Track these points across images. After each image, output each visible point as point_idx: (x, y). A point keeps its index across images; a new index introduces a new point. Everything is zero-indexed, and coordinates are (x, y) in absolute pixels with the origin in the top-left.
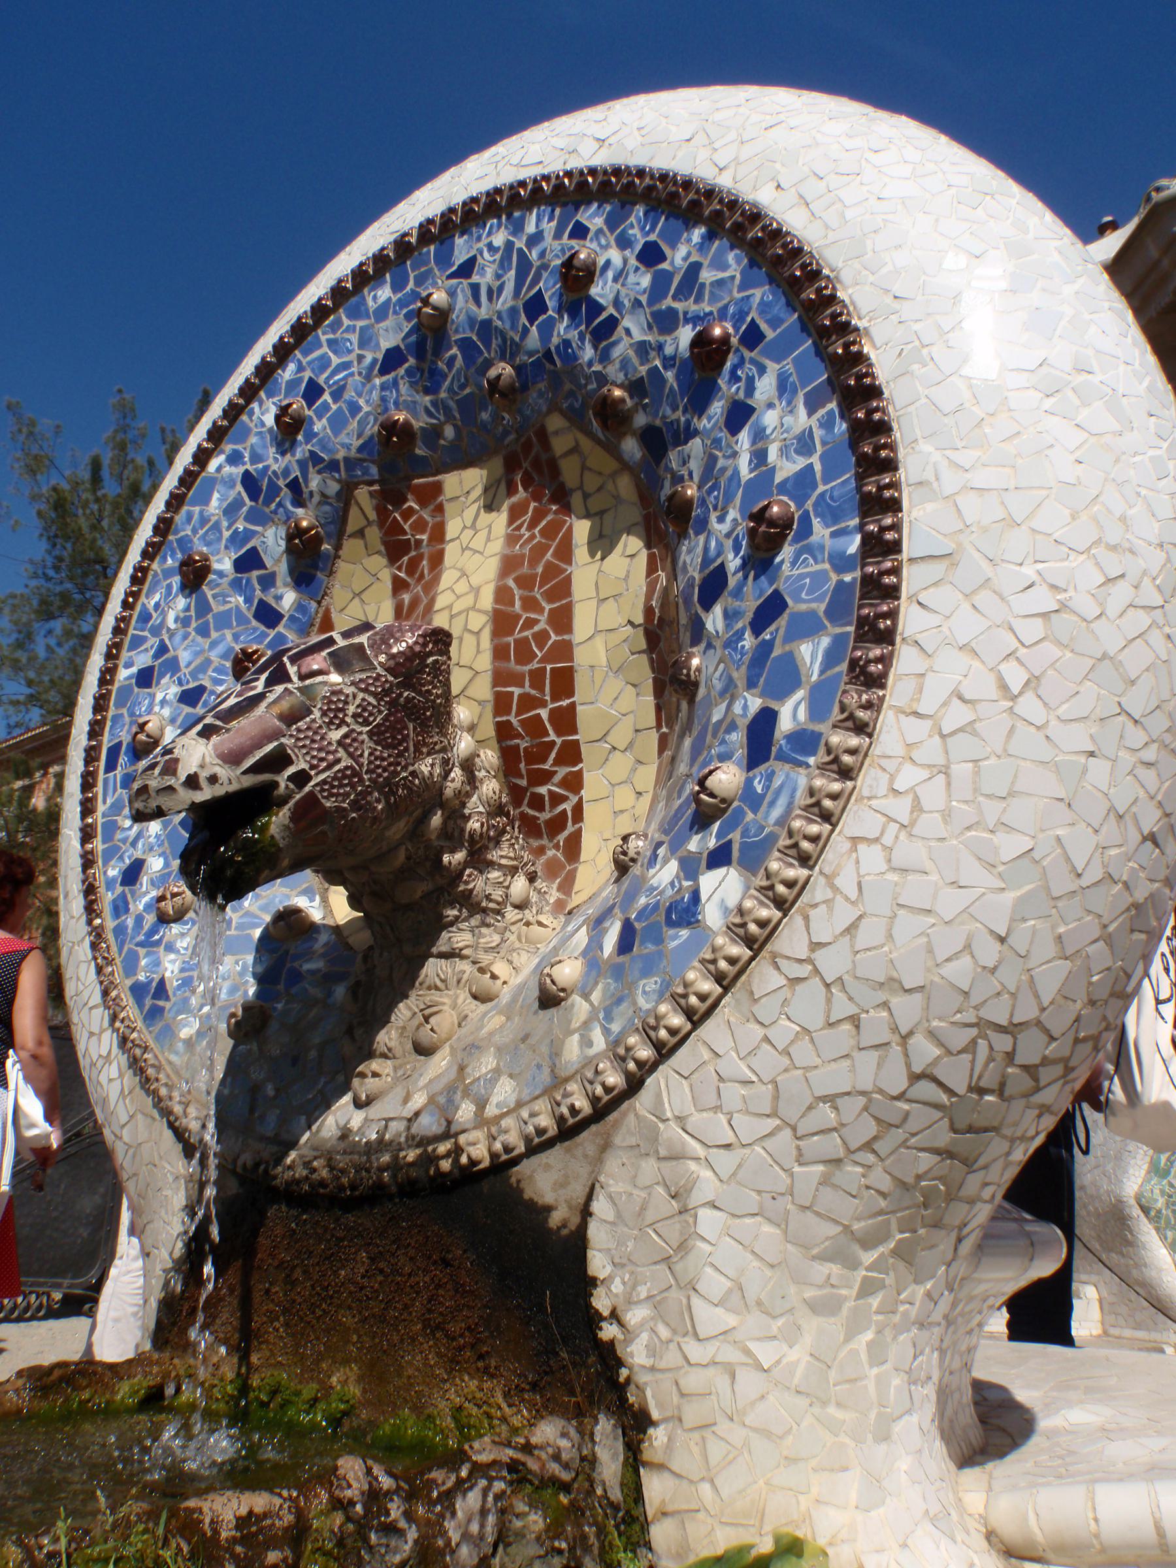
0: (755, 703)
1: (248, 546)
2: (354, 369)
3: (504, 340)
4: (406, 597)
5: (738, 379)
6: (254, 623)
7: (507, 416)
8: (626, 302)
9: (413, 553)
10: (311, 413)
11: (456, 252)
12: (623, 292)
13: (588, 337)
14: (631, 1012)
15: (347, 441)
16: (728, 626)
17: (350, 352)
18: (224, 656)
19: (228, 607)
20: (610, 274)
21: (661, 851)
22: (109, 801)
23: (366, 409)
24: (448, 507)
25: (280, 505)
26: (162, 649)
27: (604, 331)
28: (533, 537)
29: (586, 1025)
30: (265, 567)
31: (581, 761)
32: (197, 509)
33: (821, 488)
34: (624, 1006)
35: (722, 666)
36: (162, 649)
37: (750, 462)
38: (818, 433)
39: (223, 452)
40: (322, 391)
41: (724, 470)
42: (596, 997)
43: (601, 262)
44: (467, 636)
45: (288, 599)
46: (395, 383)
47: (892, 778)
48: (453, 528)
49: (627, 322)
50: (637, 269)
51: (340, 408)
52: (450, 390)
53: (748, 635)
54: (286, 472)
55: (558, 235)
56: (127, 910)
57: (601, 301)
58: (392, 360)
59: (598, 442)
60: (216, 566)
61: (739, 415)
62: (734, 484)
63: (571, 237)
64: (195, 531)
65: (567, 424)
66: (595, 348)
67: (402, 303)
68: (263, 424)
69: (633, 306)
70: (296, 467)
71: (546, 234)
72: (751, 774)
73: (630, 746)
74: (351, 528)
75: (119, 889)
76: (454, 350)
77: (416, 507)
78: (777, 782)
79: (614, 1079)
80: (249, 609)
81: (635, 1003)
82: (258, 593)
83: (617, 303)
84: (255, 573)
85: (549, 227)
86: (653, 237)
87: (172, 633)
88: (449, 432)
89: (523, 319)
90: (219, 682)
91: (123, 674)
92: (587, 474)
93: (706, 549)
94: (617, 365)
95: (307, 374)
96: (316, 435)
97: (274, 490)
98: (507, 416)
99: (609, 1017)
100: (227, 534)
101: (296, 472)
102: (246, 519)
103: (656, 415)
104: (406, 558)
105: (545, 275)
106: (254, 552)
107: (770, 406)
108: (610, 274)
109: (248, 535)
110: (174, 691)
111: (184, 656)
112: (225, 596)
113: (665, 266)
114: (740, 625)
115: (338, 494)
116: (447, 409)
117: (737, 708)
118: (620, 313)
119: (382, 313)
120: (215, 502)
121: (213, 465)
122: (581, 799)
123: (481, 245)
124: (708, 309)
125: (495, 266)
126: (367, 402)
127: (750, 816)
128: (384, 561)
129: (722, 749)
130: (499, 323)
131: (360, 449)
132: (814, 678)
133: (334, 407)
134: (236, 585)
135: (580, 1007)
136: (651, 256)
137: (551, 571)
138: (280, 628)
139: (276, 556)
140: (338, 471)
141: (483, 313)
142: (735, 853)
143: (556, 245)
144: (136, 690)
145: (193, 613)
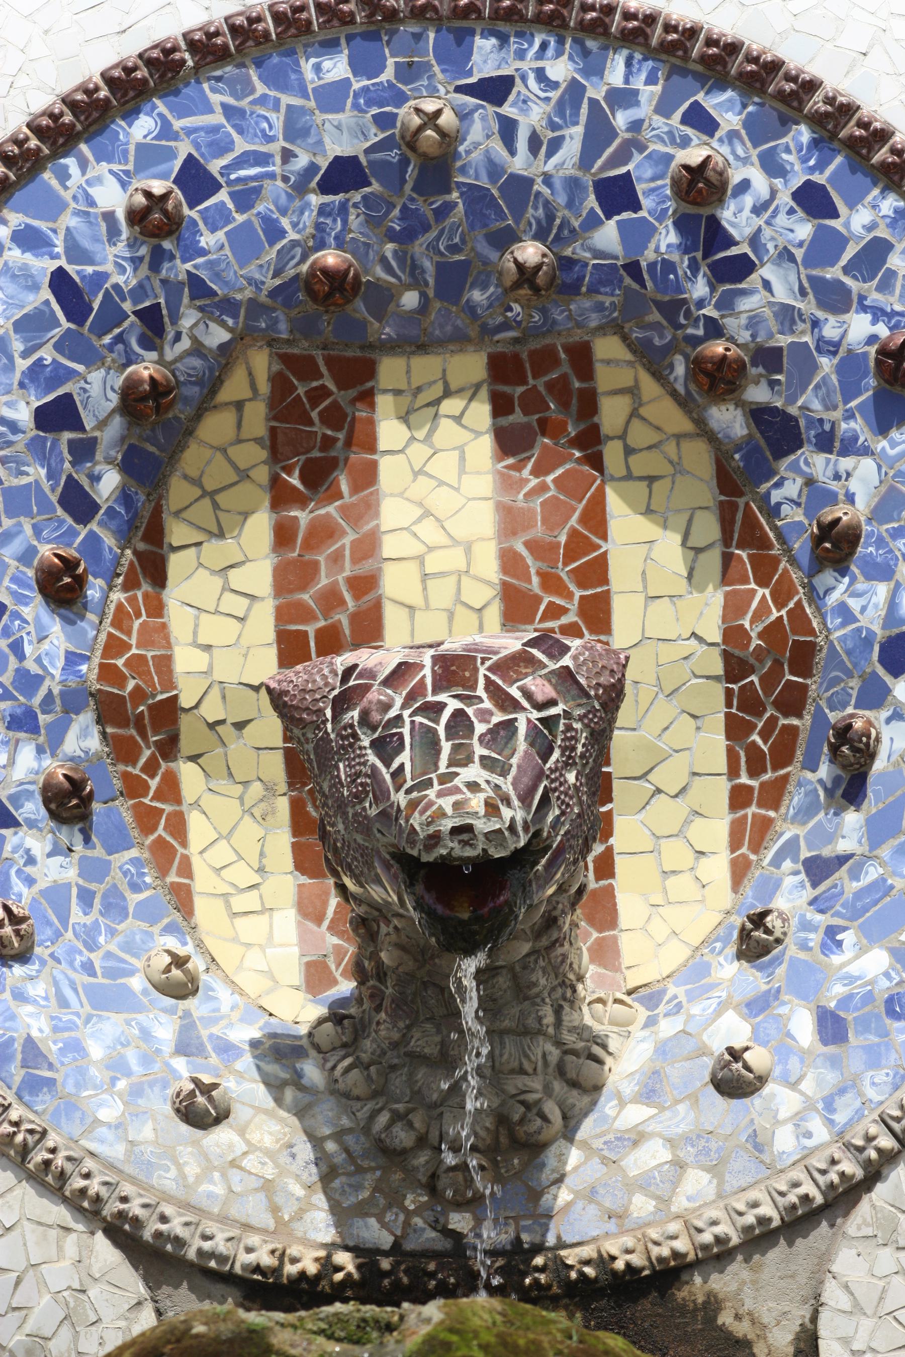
1: (60, 392)
2: (276, 167)
4: (303, 517)
6: (60, 512)
7: (517, 308)
8: (770, 246)
9: (316, 454)
10: (193, 214)
11: (476, 57)
12: (767, 233)
13: (704, 269)
14: (858, 1104)
15: (257, 276)
17: (270, 139)
18: (27, 556)
19: (25, 480)
20: (748, 200)
21: (848, 938)
23: (292, 235)
25: (119, 339)
28: (543, 488)
30: (82, 429)
31: (610, 800)
34: (849, 1096)
40: (217, 187)
42: (807, 1086)
44: (460, 610)
45: (109, 483)
46: (343, 209)
49: (767, 272)
50: (791, 212)
51: (248, 223)
52: (432, 247)
55: (664, 108)
57: (732, 230)
58: (342, 175)
59: (674, 394)
63: (685, 121)
65: (629, 356)
66: (713, 289)
67: (371, 97)
68: (92, 203)
69: (780, 255)
71: (643, 98)
73: (683, 790)
74: (226, 394)
77: (331, 386)
79: (850, 1167)
80: (53, 490)
81: (860, 1094)
82: (67, 465)
83: (755, 240)
84: (67, 435)
85: (649, 94)
86: (820, 178)
88: (410, 299)
89: (591, 202)
90: (21, 600)
92: (636, 424)
94: (743, 320)
95: (184, 149)
96: (203, 252)
97: (112, 315)
98: (517, 308)
99: (829, 1104)
100: (22, 364)
102: (58, 347)
103: (792, 400)
104: (303, 458)
105: (637, 158)
106: (68, 397)
109: (61, 375)
112: (19, 463)
115: (224, 348)
118: (760, 260)
119: (332, 97)
122: (609, 851)
123: (525, 66)
125: (549, 108)
126: (295, 225)
128: (264, 454)
130: (546, 191)
131: (274, 293)
133: (240, 218)
134: (35, 446)
135: (779, 1099)
136: (813, 201)
137: (578, 545)
138: (94, 526)
139: (102, 415)
140: (235, 316)
141: (519, 163)
143: (658, 121)
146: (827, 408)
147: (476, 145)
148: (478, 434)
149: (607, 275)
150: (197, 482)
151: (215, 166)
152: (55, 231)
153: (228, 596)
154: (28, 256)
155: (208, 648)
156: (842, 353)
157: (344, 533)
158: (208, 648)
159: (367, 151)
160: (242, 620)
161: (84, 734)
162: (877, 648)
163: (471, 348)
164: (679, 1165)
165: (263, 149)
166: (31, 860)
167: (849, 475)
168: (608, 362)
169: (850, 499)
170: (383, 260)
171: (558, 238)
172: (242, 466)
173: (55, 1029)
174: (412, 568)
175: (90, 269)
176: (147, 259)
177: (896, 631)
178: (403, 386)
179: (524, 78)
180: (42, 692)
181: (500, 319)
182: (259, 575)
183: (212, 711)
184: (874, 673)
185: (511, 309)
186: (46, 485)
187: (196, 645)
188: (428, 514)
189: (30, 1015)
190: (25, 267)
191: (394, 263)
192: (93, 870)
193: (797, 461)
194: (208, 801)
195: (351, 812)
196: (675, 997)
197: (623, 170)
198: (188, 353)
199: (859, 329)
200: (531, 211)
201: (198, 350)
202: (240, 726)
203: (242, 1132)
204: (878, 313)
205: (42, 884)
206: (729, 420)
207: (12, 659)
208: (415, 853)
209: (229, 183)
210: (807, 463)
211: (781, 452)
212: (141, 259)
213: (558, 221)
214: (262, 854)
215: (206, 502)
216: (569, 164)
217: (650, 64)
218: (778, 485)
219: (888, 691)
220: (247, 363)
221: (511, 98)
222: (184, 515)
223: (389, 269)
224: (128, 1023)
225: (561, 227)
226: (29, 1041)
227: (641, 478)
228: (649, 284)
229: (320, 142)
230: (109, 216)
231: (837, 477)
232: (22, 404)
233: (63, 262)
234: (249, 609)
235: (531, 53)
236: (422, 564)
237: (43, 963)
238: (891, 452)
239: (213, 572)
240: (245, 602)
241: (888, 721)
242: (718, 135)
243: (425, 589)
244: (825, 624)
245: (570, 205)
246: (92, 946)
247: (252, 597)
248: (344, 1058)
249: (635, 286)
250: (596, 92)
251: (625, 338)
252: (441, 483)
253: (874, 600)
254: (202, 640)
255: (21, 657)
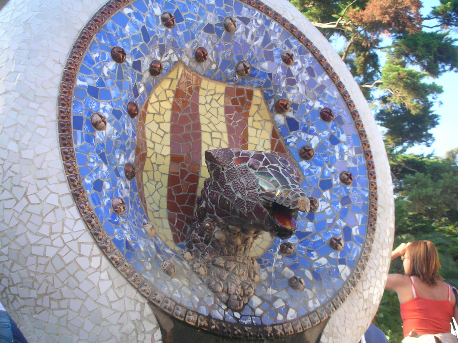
0: (344, 224)
3: (252, 56)
5: (334, 130)
6: (132, 93)
7: (237, 77)
8: (300, 79)
11: (242, 12)
12: (300, 76)
16: (331, 198)
17: (196, 13)
19: (128, 80)
21: (314, 253)
22: (79, 144)
24: (201, 90)
26: (101, 83)
27: (292, 82)
29: (313, 298)
30: (141, 71)
32: (118, 26)
33: (359, 176)
35: (329, 209)
36: (101, 83)
37: (339, 156)
38: (358, 160)
39: (132, 9)
40: (182, 20)
41: (330, 153)
43: (295, 61)
47: (376, 256)
48: (202, 100)
49: (298, 85)
51: (188, 32)
53: (340, 204)
54: (161, 40)
56: (100, 203)
57: (293, 73)
58: (209, 29)
59: (268, 109)
60: (127, 59)
61: (334, 140)
62: (334, 160)
64: (116, 34)
65: (261, 97)
68: (153, 12)
70: (166, 41)
72: (346, 242)
74: (171, 76)
75: (94, 191)
76: (230, 43)
78: (354, 247)
84: (138, 72)
86: (313, 67)
87: (106, 79)
88: (214, 66)
90: (125, 113)
91: (79, 83)
92: (257, 114)
93: (323, 172)
94: (292, 95)
95: (177, 7)
96: (178, 36)
100: (133, 48)
101: (165, 43)
105: (274, 48)
106: (139, 62)
107: (345, 144)
108: (297, 67)
110: (109, 107)
111: (113, 93)
113: (314, 78)
114: (337, 200)
115: (175, 63)
116: (218, 59)
117: (338, 222)
120: (127, 28)
121: (127, 11)
124: (326, 102)
126: (197, 37)
127: (348, 254)
129: (334, 232)
132: (360, 224)
133: (187, 30)
136: (310, 71)
139: (145, 70)
141: (248, 40)
142: (347, 262)
143: (280, 41)
144: (88, 95)
145: (116, 74)
146: (307, 122)
147: (239, 33)
148: (221, 106)
149: (263, 74)
150: (157, 97)
151: (183, 14)
152: (144, 16)
153: (159, 130)
154: (137, 20)
155: (154, 143)
156: (312, 109)
157: (190, 121)
158: (154, 143)
159: (216, 25)
160: (162, 137)
161: (132, 157)
162: (319, 183)
163: (222, 84)
164: (287, 308)
165: (194, 14)
166: (122, 188)
167: (311, 139)
168: (256, 96)
169: (311, 145)
170: (212, 53)
171: (253, 62)
172: (168, 96)
173: (132, 239)
174: (208, 135)
175: (151, 30)
176: (164, 32)
177: (324, 179)
178: (206, 88)
179: (252, 20)
180: (127, 141)
181: (232, 78)
182: (167, 127)
183: (153, 159)
184: (317, 188)
185: (235, 76)
186: (131, 83)
187: (151, 140)
188: (210, 122)
189: (126, 234)
190: (136, 22)
191: (214, 56)
192: (132, 195)
193: (297, 133)
194: (148, 184)
195: (247, 192)
196: (266, 262)
197: (271, 50)
198: (167, 61)
199: (317, 105)
200: (248, 53)
201: (169, 61)
202: (159, 166)
203: (179, 279)
204: (322, 103)
205: (124, 196)
206: (280, 119)
207: (122, 129)
208: (287, 206)
209: (186, 20)
210: (299, 134)
211: (291, 130)
212: (163, 31)
213: (254, 58)
214: (160, 202)
215: (158, 103)
216: (259, 45)
217: (279, 27)
218: (290, 138)
219: (322, 194)
220: (178, 69)
221: (249, 24)
222: (154, 105)
223: (212, 57)
224: (145, 241)
225: (254, 60)
226: (127, 241)
227: (255, 128)
228: (273, 80)
229: (206, 18)
230: (157, 17)
231: (307, 139)
232: (131, 59)
233: (145, 25)
234: (164, 135)
235: (254, 15)
236: (211, 135)
237: (126, 219)
238: (323, 136)
239: (156, 123)
240: (163, 133)
241: (321, 201)
242: (292, 49)
243: (212, 141)
244: (303, 174)
245: (258, 55)
246: (134, 218)
247: (165, 133)
248: (194, 263)
249: (269, 79)
250: (267, 29)
251: (262, 91)
252: (213, 116)
253: (318, 170)
254: (152, 140)
255: (124, 129)
